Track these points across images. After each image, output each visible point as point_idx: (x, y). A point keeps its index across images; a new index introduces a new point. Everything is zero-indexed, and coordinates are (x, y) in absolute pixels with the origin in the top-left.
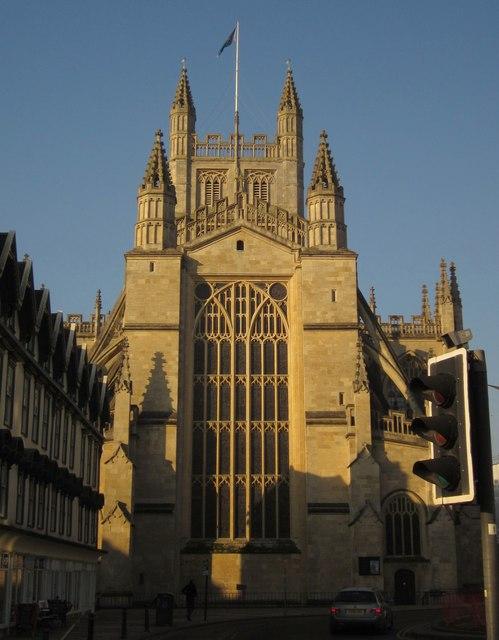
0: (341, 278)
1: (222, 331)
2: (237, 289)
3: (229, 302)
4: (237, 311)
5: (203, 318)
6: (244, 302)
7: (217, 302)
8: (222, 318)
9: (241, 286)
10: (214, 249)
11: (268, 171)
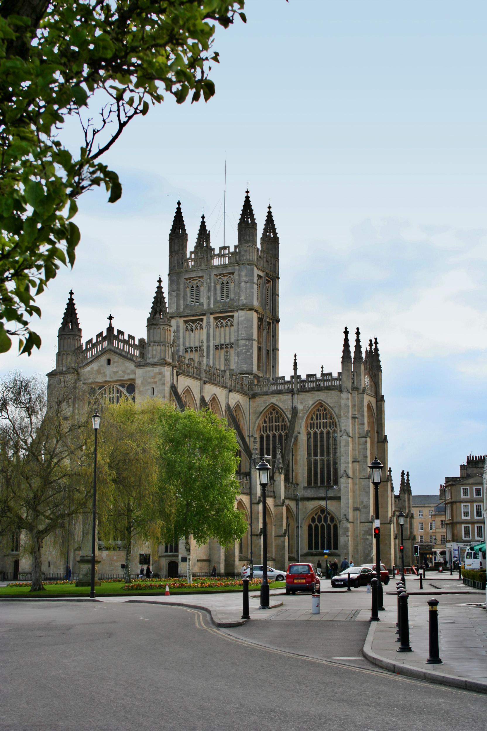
0: (157, 380)
9: (111, 387)
10: (94, 366)
11: (230, 273)
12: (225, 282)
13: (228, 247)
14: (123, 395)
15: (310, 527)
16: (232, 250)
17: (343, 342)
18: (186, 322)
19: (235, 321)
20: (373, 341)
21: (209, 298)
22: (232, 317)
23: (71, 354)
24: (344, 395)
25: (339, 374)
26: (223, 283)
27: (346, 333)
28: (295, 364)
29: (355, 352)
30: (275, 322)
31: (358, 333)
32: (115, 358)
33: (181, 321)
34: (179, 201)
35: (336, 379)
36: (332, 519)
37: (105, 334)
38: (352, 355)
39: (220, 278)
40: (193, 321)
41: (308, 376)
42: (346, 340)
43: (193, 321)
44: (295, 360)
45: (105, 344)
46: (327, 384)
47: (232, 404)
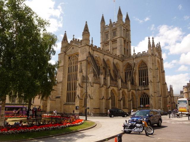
13: (115, 22)
15: (140, 98)
16: (116, 23)
20: (158, 43)
21: (110, 36)
22: (116, 40)
24: (149, 57)
25: (148, 51)
28: (134, 50)
35: (147, 53)
36: (148, 96)
38: (151, 45)
40: (107, 43)
41: (138, 53)
42: (149, 41)
43: (107, 43)
47: (115, 62)
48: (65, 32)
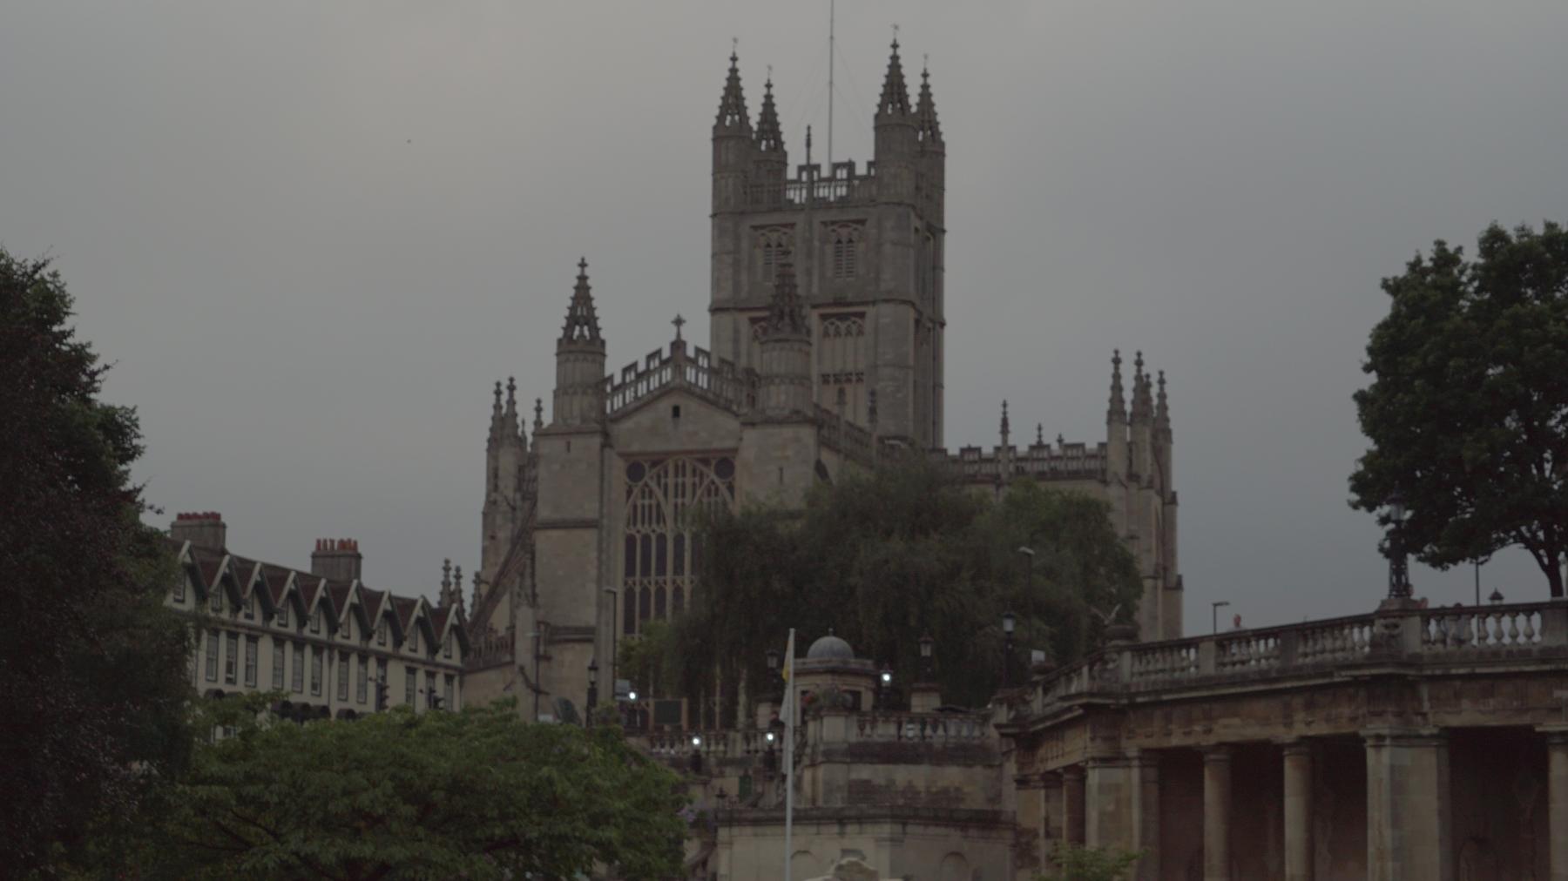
1: (658, 522)
2: (676, 467)
3: (666, 485)
4: (676, 496)
5: (635, 507)
6: (684, 485)
7: (653, 485)
8: (658, 505)
9: (680, 463)
10: (644, 419)
12: (844, 239)
13: (850, 166)
14: (706, 482)
16: (861, 170)
17: (1110, 381)
18: (753, 321)
19: (868, 324)
21: (809, 272)
22: (862, 315)
23: (590, 391)
26: (839, 242)
27: (1117, 361)
28: (1005, 423)
29: (1133, 402)
30: (938, 327)
31: (1139, 363)
32: (690, 406)
33: (743, 319)
34: (734, 54)
37: (666, 354)
38: (1128, 408)
39: (834, 231)
42: (1117, 377)
44: (1005, 413)
45: (667, 375)
46: (1073, 465)
48: (583, 265)
